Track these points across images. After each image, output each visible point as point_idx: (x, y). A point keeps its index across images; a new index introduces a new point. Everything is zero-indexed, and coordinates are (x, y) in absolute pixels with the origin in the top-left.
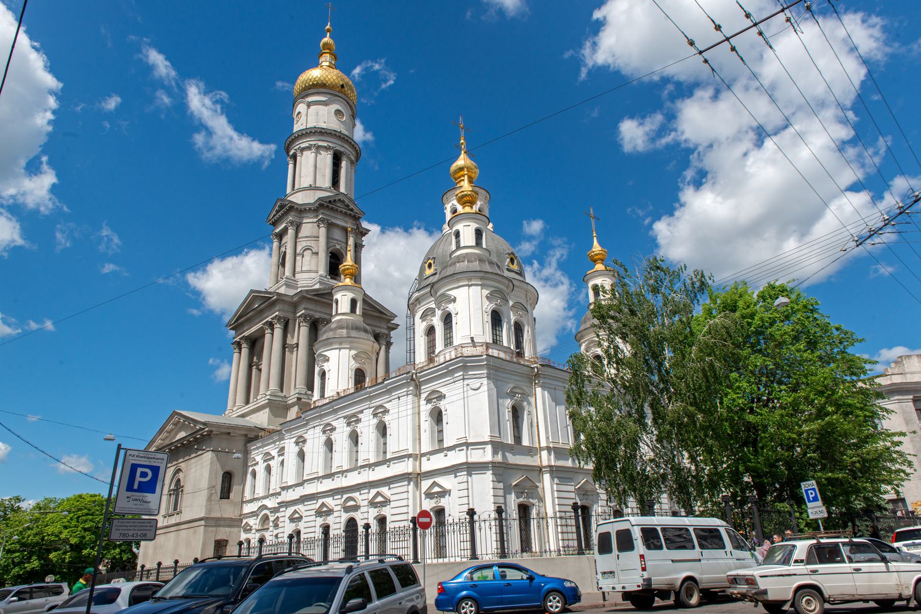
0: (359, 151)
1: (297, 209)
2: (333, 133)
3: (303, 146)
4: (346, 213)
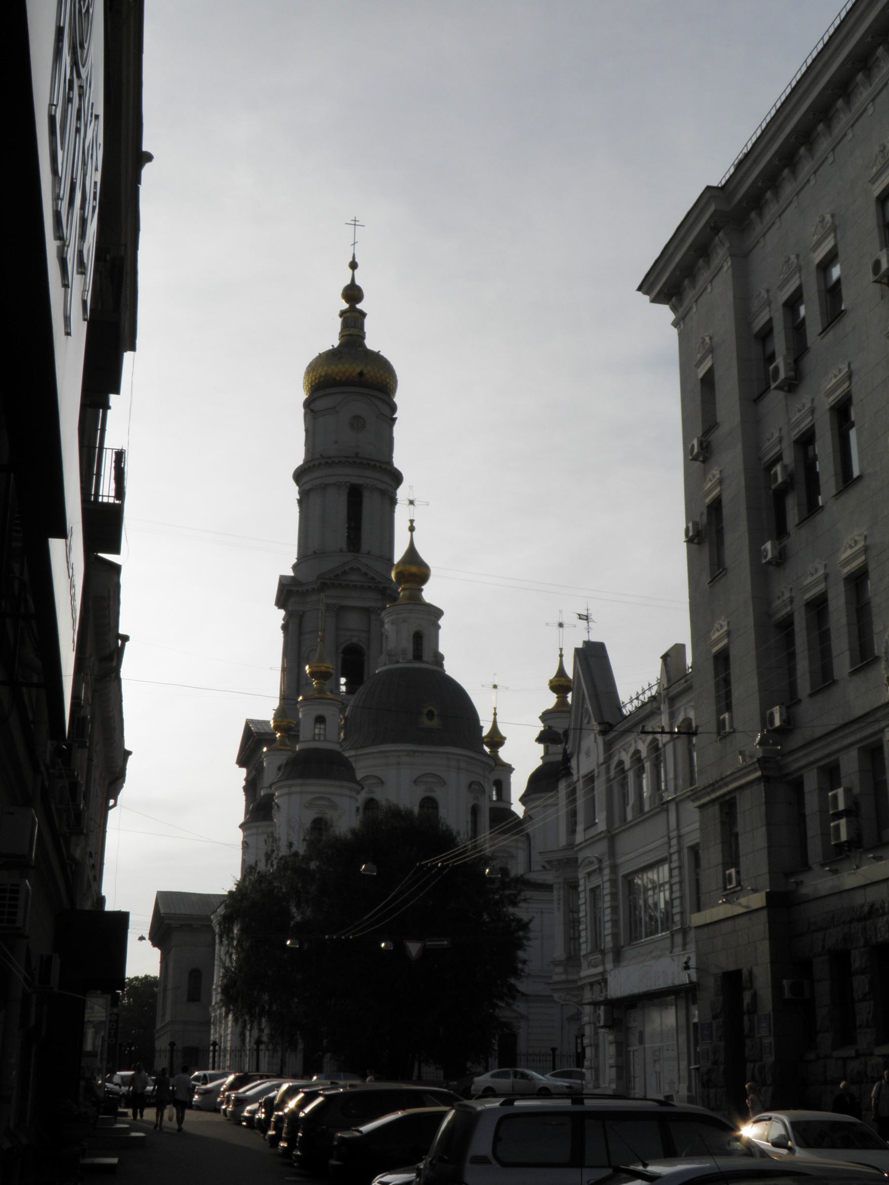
1: (298, 591)
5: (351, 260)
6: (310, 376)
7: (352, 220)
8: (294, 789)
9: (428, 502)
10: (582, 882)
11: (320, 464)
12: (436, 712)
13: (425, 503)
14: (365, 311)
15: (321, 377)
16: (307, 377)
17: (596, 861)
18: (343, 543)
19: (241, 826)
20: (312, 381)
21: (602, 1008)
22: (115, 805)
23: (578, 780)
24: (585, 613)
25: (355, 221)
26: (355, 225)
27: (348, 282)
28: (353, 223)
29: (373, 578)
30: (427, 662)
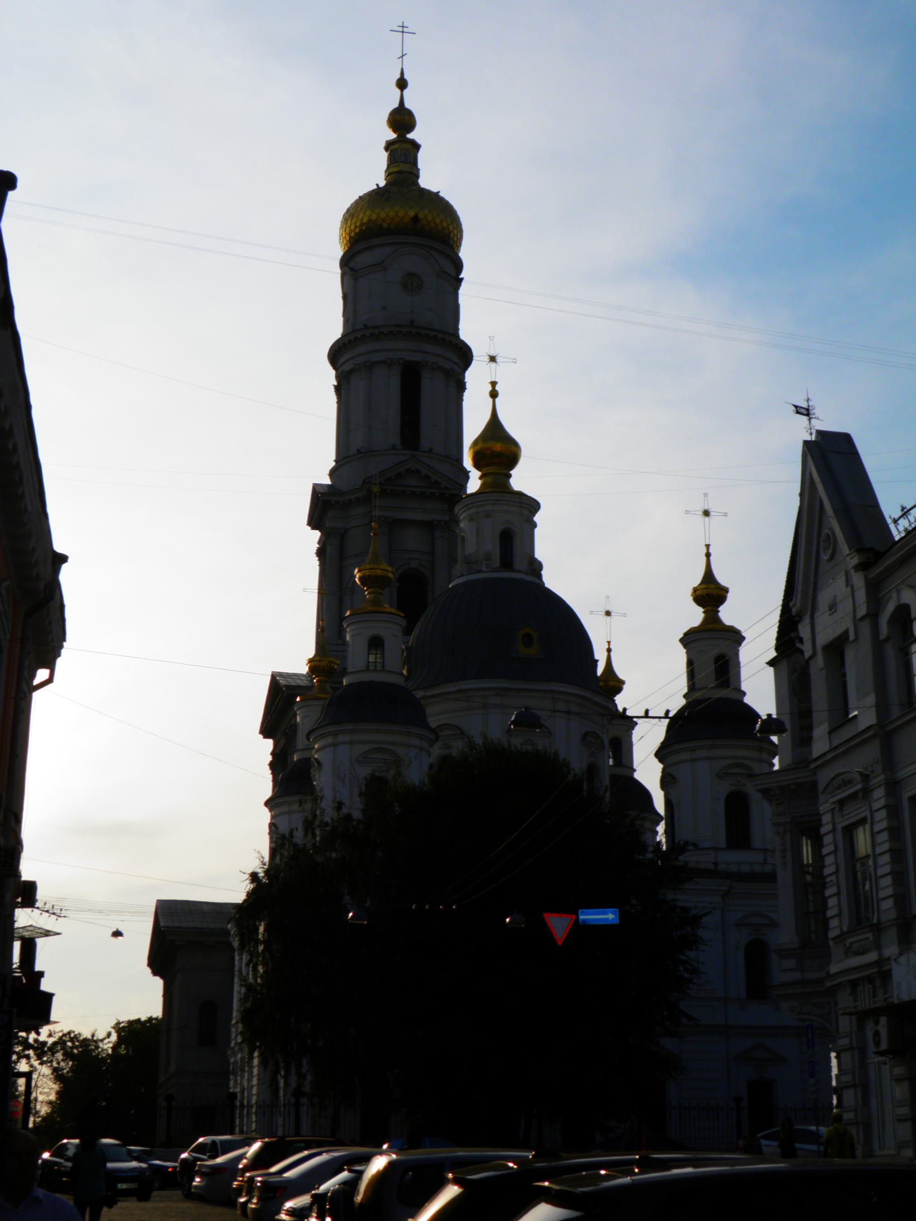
5: (398, 76)
6: (349, 224)
7: (399, 26)
8: (340, 738)
10: (826, 819)
11: (364, 336)
13: (511, 360)
14: (419, 141)
15: (362, 224)
16: (345, 226)
17: (858, 778)
18: (396, 439)
19: (267, 804)
20: (351, 231)
21: (883, 1020)
22: (50, 680)
23: (814, 655)
24: (805, 405)
25: (403, 27)
26: (403, 32)
27: (396, 105)
28: (401, 29)
30: (519, 571)
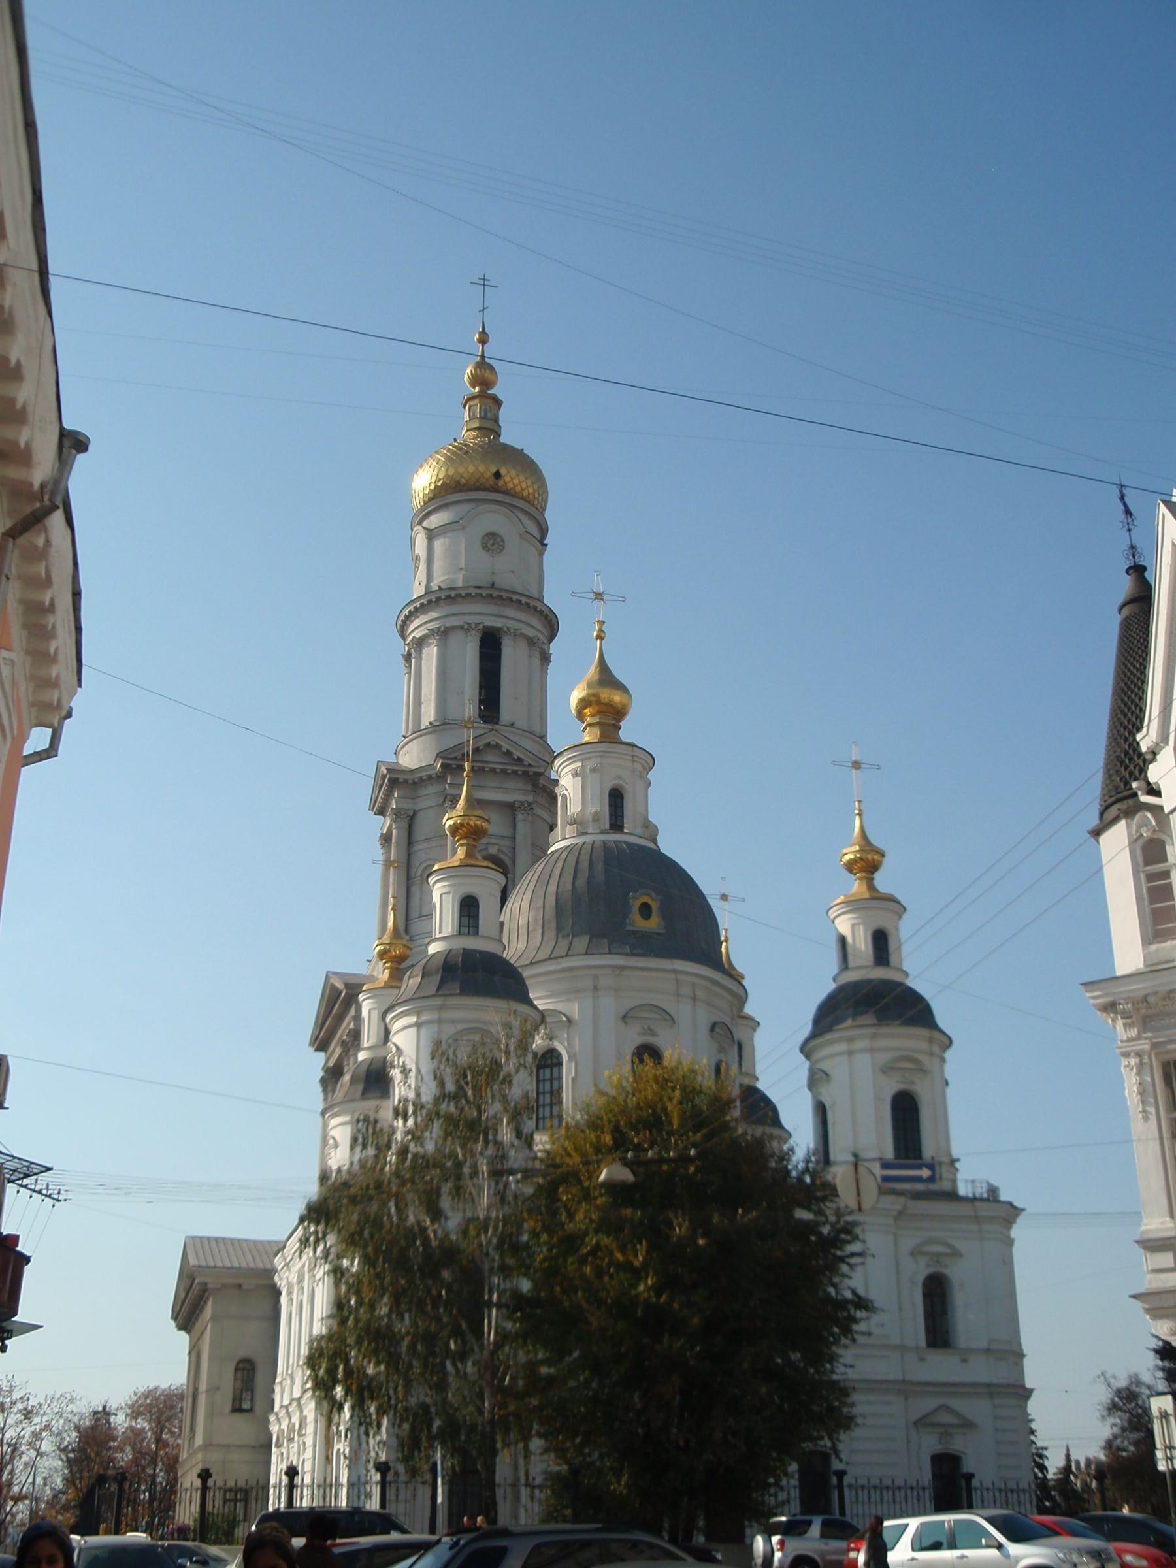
0: (546, 611)
1: (406, 781)
2: (473, 592)
3: (418, 634)
4: (504, 771)
7: (480, 279)
9: (624, 598)
12: (654, 905)
25: (484, 279)
28: (482, 282)
29: (519, 759)
